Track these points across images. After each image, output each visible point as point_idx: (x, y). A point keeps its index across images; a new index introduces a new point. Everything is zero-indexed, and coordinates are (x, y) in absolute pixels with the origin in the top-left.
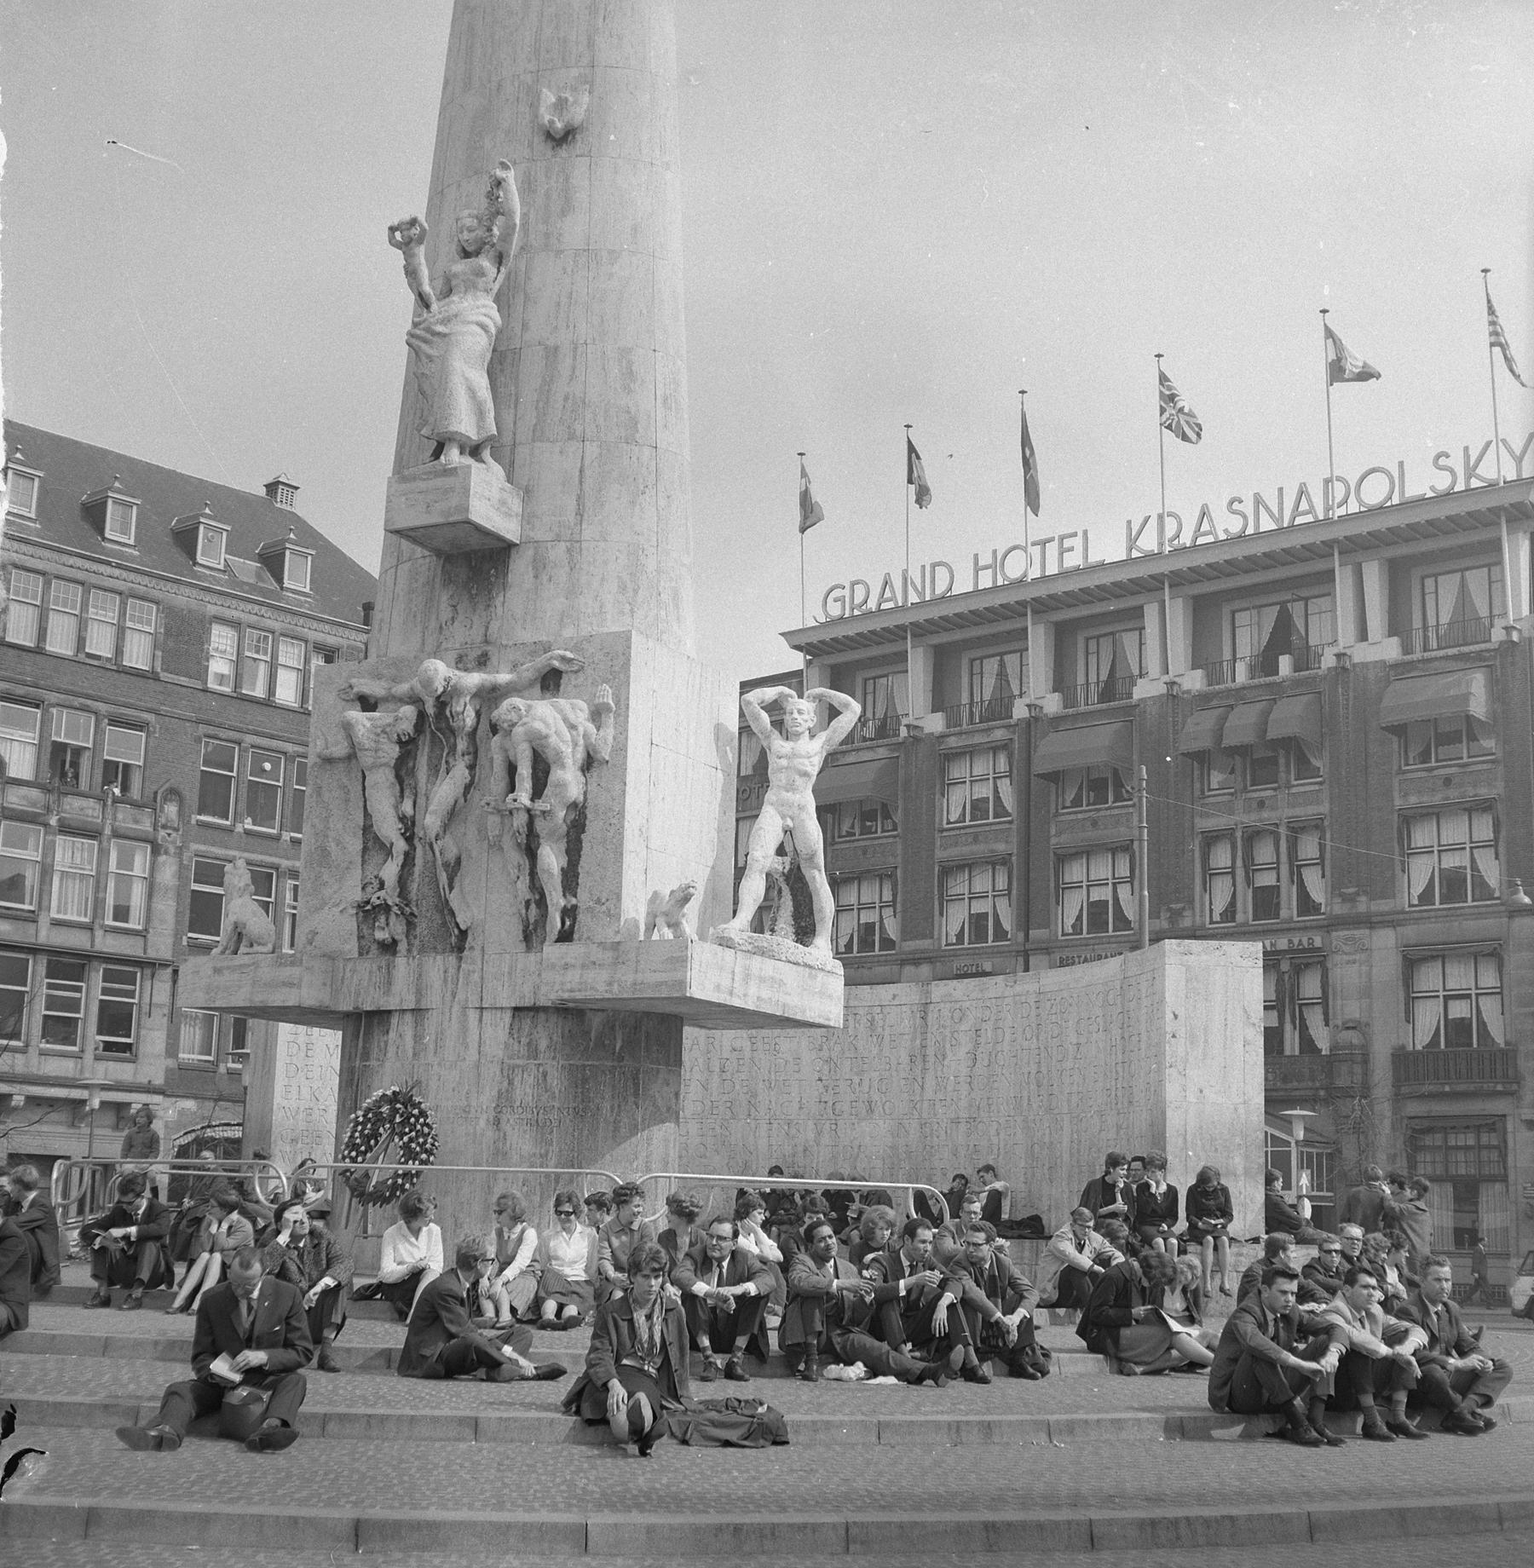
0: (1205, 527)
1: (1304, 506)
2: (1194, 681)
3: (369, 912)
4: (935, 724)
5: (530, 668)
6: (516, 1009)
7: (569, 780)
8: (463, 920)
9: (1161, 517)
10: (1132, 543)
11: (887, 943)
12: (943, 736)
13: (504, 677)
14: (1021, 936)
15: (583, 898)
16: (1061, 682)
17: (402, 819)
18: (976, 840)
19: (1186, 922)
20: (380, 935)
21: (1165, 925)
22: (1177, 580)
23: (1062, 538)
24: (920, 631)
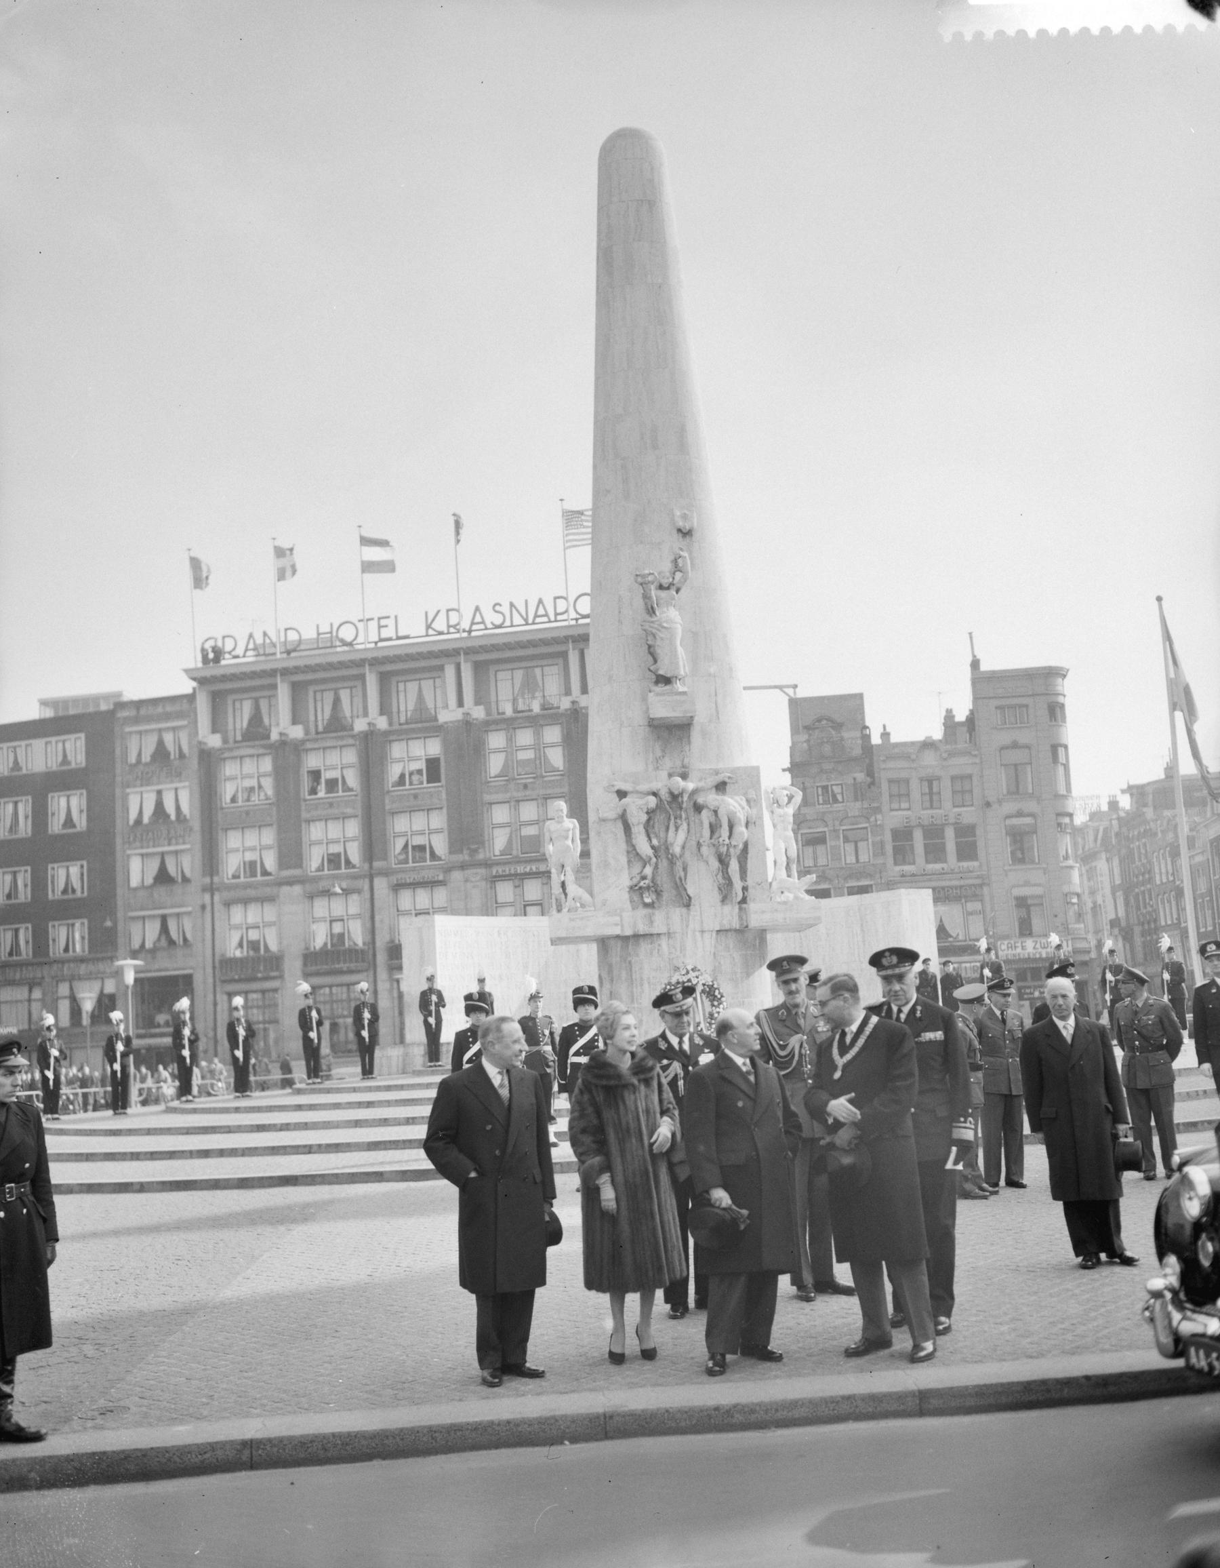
0: (478, 619)
1: (541, 611)
2: (479, 713)
3: (636, 890)
4: (297, 732)
5: (712, 781)
6: (718, 931)
7: (741, 831)
8: (690, 892)
9: (448, 611)
10: (428, 627)
11: (265, 873)
12: (303, 742)
13: (701, 784)
14: (366, 866)
15: (750, 882)
16: (384, 709)
17: (653, 847)
18: (331, 805)
19: (481, 856)
20: (648, 900)
21: (467, 858)
22: (469, 651)
23: (379, 619)
24: (285, 672)
